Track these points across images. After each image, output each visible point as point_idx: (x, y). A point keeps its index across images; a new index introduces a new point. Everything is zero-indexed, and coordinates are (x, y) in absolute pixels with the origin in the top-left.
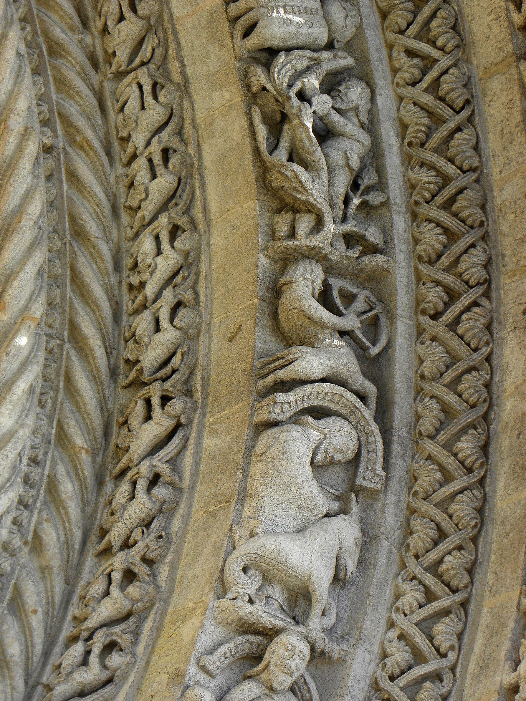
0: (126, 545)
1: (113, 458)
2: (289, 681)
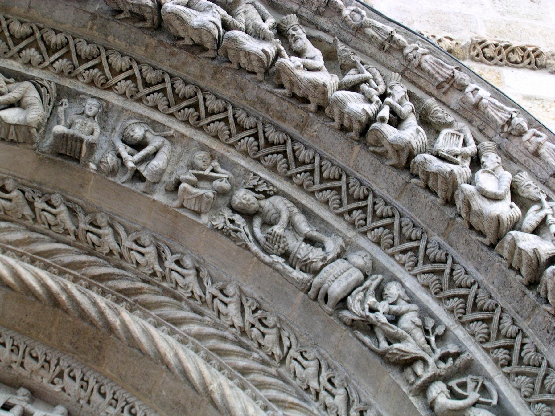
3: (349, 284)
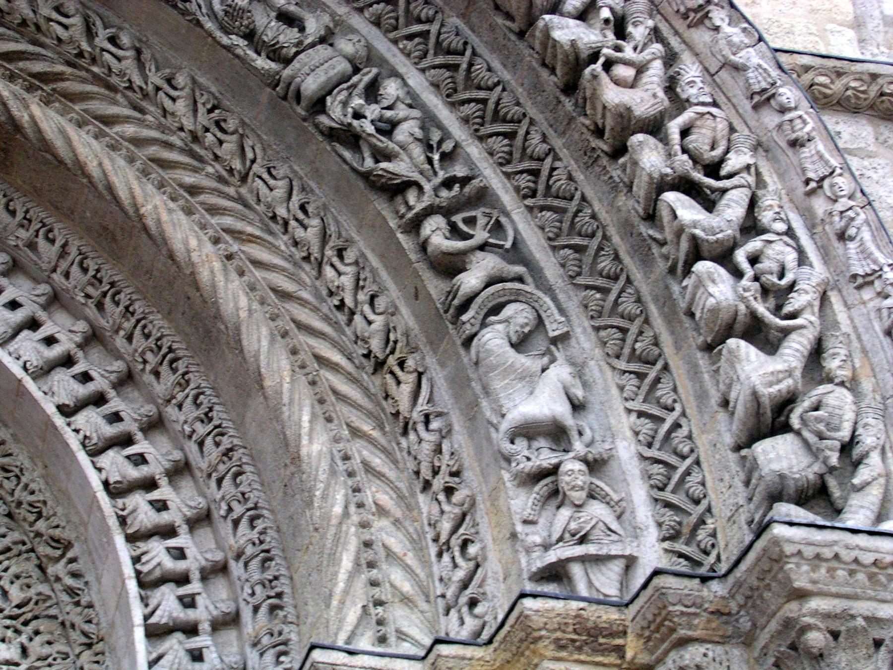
0: (436, 472)
2: (583, 494)
3: (329, 79)
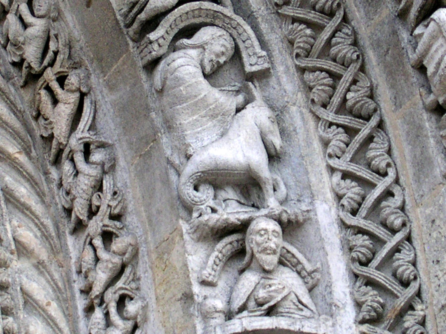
1: (45, 148)
2: (275, 259)
